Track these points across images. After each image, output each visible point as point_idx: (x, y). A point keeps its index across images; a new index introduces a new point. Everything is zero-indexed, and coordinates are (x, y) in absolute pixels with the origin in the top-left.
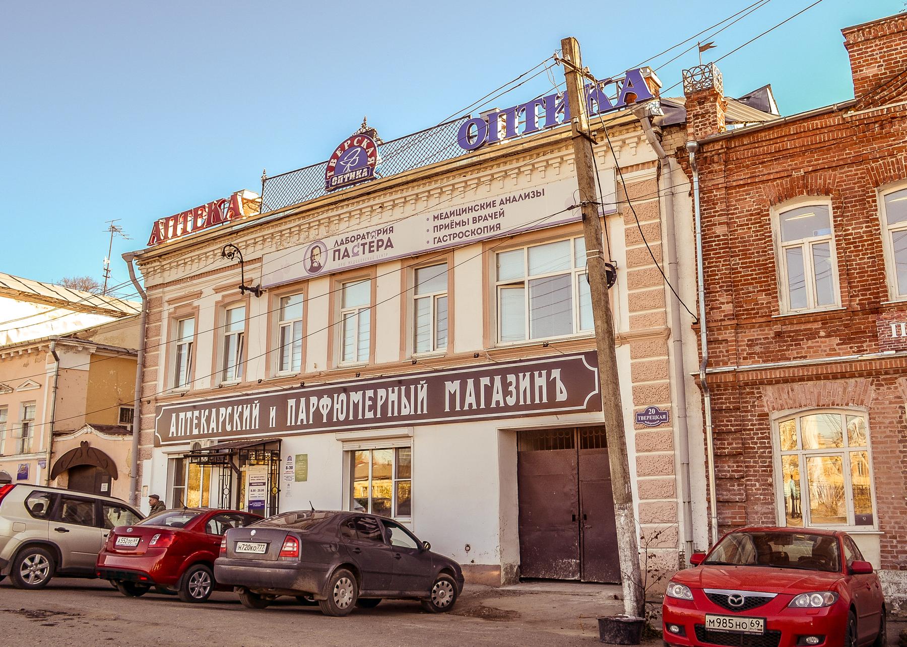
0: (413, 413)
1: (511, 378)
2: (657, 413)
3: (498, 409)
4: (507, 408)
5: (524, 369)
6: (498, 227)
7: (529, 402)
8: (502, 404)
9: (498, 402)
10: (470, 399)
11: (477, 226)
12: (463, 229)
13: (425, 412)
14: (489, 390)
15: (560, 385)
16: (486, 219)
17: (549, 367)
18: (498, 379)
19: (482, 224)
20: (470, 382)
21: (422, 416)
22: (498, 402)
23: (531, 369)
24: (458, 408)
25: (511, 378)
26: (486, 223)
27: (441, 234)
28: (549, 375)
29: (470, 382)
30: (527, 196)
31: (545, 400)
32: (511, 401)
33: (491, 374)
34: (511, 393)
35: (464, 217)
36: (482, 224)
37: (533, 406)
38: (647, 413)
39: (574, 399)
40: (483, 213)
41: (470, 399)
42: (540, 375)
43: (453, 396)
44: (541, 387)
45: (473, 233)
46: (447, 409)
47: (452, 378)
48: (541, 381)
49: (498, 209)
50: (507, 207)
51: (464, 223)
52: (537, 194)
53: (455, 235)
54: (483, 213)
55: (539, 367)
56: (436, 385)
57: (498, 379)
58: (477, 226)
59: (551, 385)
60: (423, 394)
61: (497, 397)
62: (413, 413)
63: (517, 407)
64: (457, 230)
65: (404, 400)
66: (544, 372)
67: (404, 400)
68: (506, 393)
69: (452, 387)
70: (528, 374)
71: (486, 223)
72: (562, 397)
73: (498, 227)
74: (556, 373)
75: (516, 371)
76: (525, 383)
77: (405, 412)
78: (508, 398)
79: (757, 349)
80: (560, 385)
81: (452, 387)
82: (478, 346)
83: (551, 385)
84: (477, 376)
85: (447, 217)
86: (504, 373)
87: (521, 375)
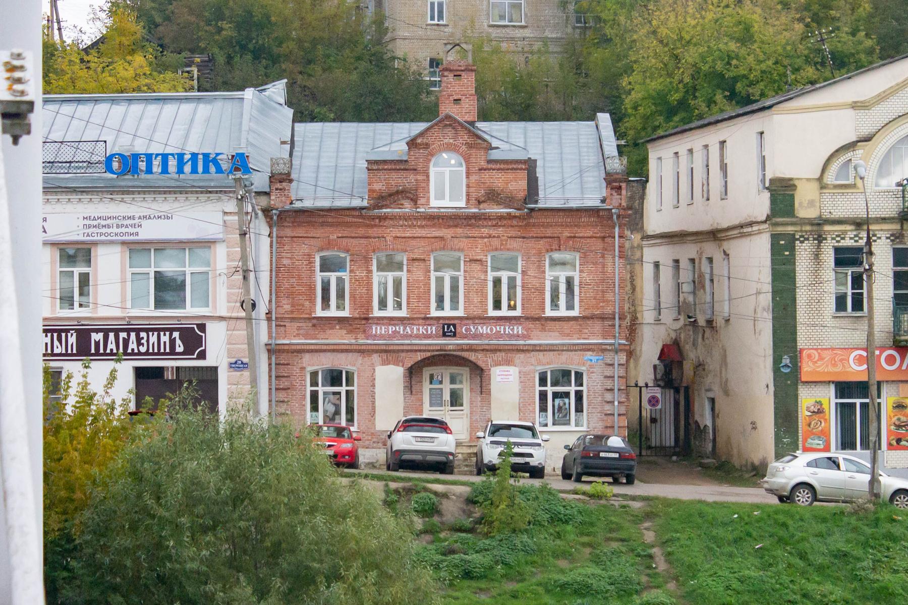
0: (64, 352)
1: (143, 334)
2: (242, 363)
3: (133, 353)
4: (140, 353)
5: (153, 330)
6: (137, 234)
7: (156, 351)
8: (136, 351)
9: (133, 350)
10: (111, 346)
11: (119, 230)
12: (109, 231)
13: (75, 351)
14: (126, 342)
15: (178, 342)
16: (127, 227)
17: (171, 330)
18: (133, 335)
19: (124, 230)
20: (112, 336)
21: (72, 355)
22: (133, 350)
23: (158, 330)
24: (102, 351)
25: (143, 334)
26: (127, 230)
27: (90, 231)
28: (171, 335)
29: (112, 336)
30: (159, 217)
31: (168, 350)
32: (143, 349)
33: (128, 331)
34: (143, 345)
35: (109, 222)
36: (124, 230)
37: (159, 354)
38: (236, 363)
39: (188, 351)
40: (125, 222)
41: (111, 346)
42: (165, 335)
43: (97, 344)
44: (165, 343)
45: (116, 235)
46: (93, 351)
47: (97, 331)
48: (165, 338)
49: (137, 221)
50: (144, 223)
51: (109, 227)
52: (168, 218)
53: (101, 234)
54: (125, 222)
55: (165, 330)
56: (84, 335)
57: (133, 335)
58: (119, 230)
59: (172, 342)
60: (72, 340)
61: (133, 345)
62: (64, 352)
63: (147, 353)
64: (104, 230)
65: (56, 343)
66: (167, 333)
67: (56, 343)
68: (139, 344)
69: (97, 337)
70: (156, 333)
71: (127, 230)
72: (180, 348)
73: (137, 234)
74: (176, 334)
75: (147, 331)
76: (153, 339)
77: (56, 351)
78: (141, 348)
79: (301, 332)
80: (178, 342)
81: (97, 337)
82: (118, 313)
83: (172, 342)
84: (117, 332)
85: (94, 219)
86: (138, 331)
87: (151, 334)
